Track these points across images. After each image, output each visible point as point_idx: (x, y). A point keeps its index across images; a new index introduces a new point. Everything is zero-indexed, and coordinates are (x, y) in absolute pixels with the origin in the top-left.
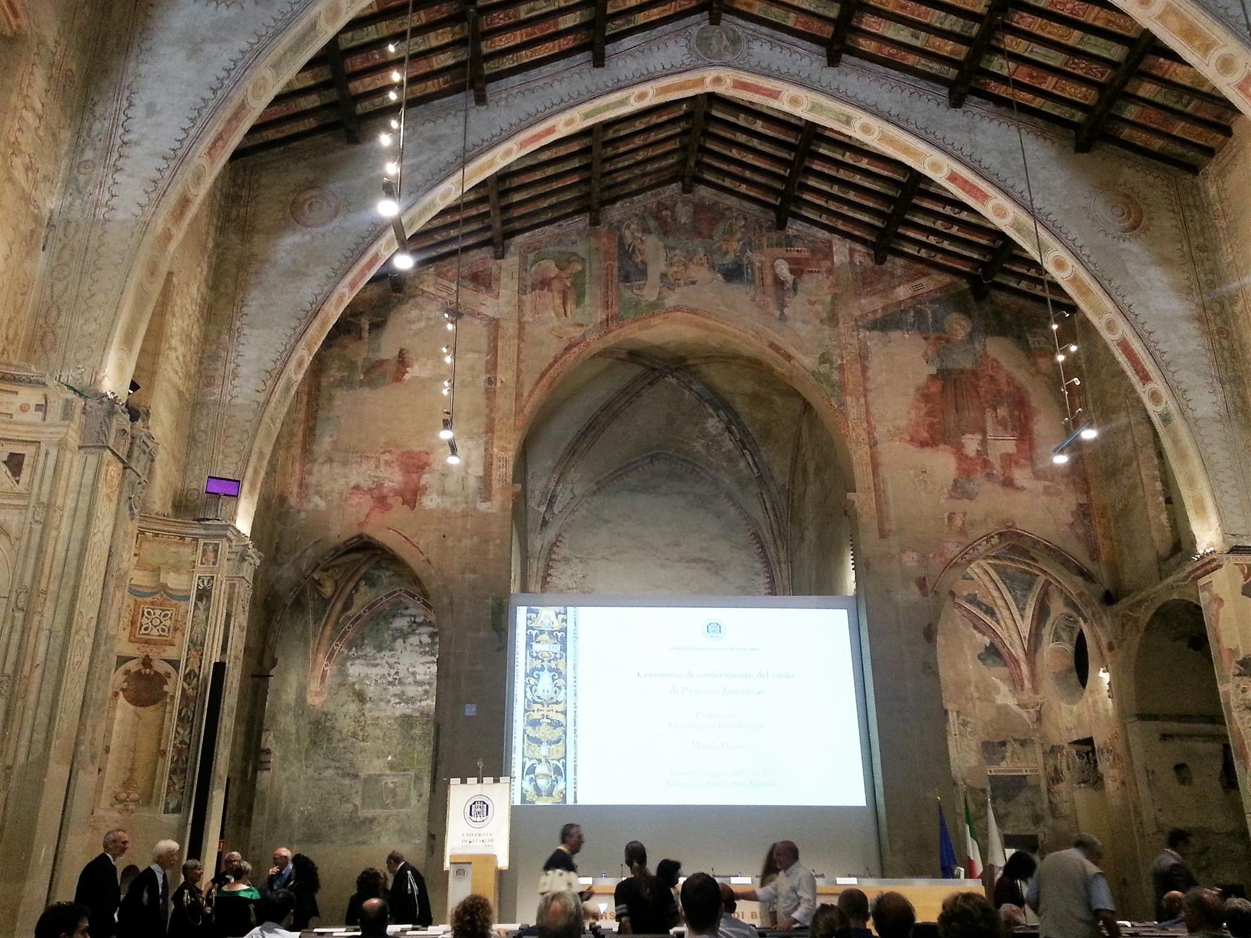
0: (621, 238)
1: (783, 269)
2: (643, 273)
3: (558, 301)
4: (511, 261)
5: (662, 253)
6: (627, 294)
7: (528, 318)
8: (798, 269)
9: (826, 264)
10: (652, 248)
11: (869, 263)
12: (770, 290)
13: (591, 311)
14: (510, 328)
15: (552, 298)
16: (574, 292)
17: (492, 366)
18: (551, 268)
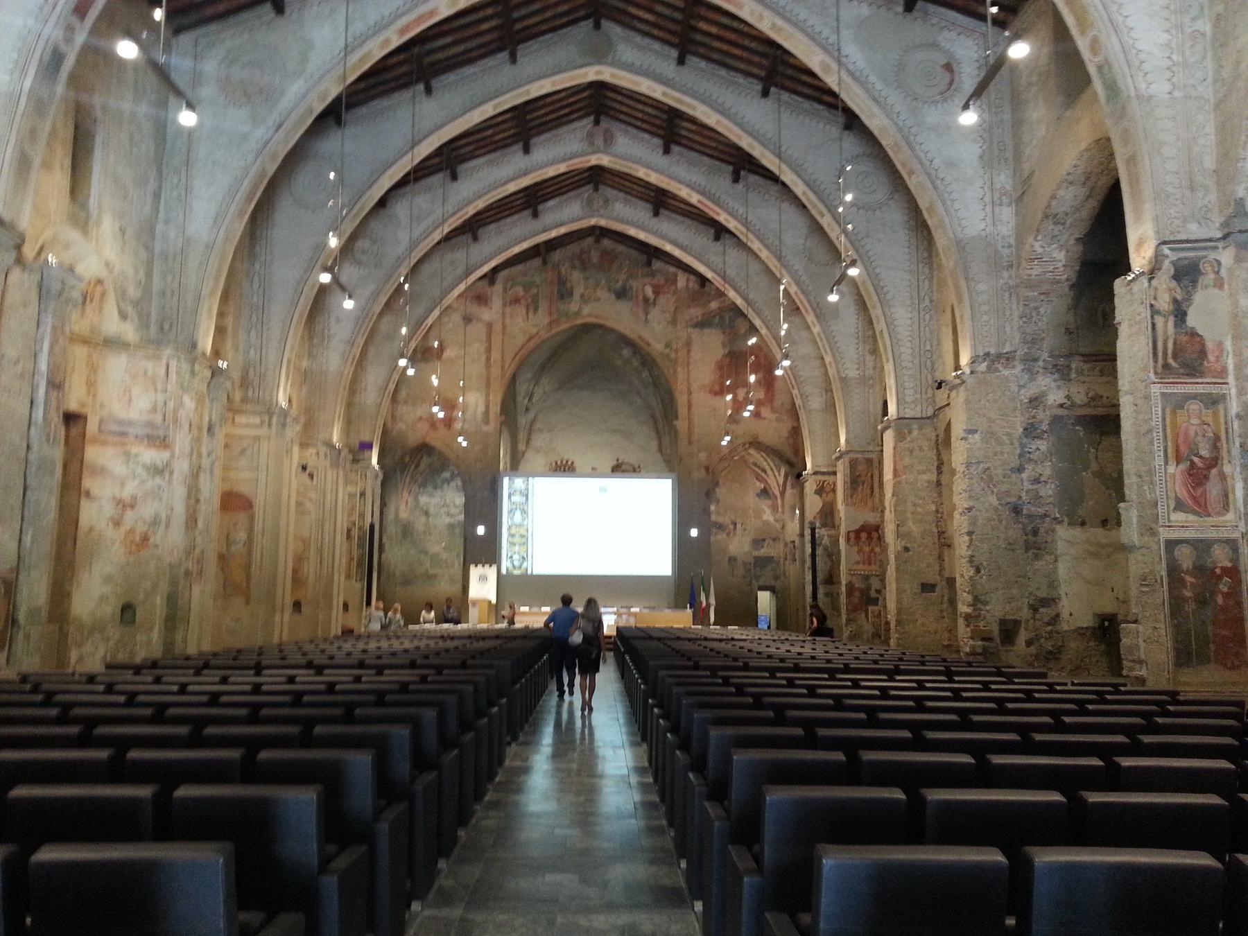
0: (559, 272)
1: (649, 291)
2: (571, 294)
3: (524, 311)
4: (498, 287)
5: (582, 282)
6: (562, 307)
7: (507, 321)
8: (657, 293)
9: (673, 288)
10: (576, 277)
11: (697, 287)
12: (641, 303)
13: (542, 318)
14: (498, 327)
15: (520, 310)
16: (533, 306)
17: (489, 351)
18: (520, 291)
